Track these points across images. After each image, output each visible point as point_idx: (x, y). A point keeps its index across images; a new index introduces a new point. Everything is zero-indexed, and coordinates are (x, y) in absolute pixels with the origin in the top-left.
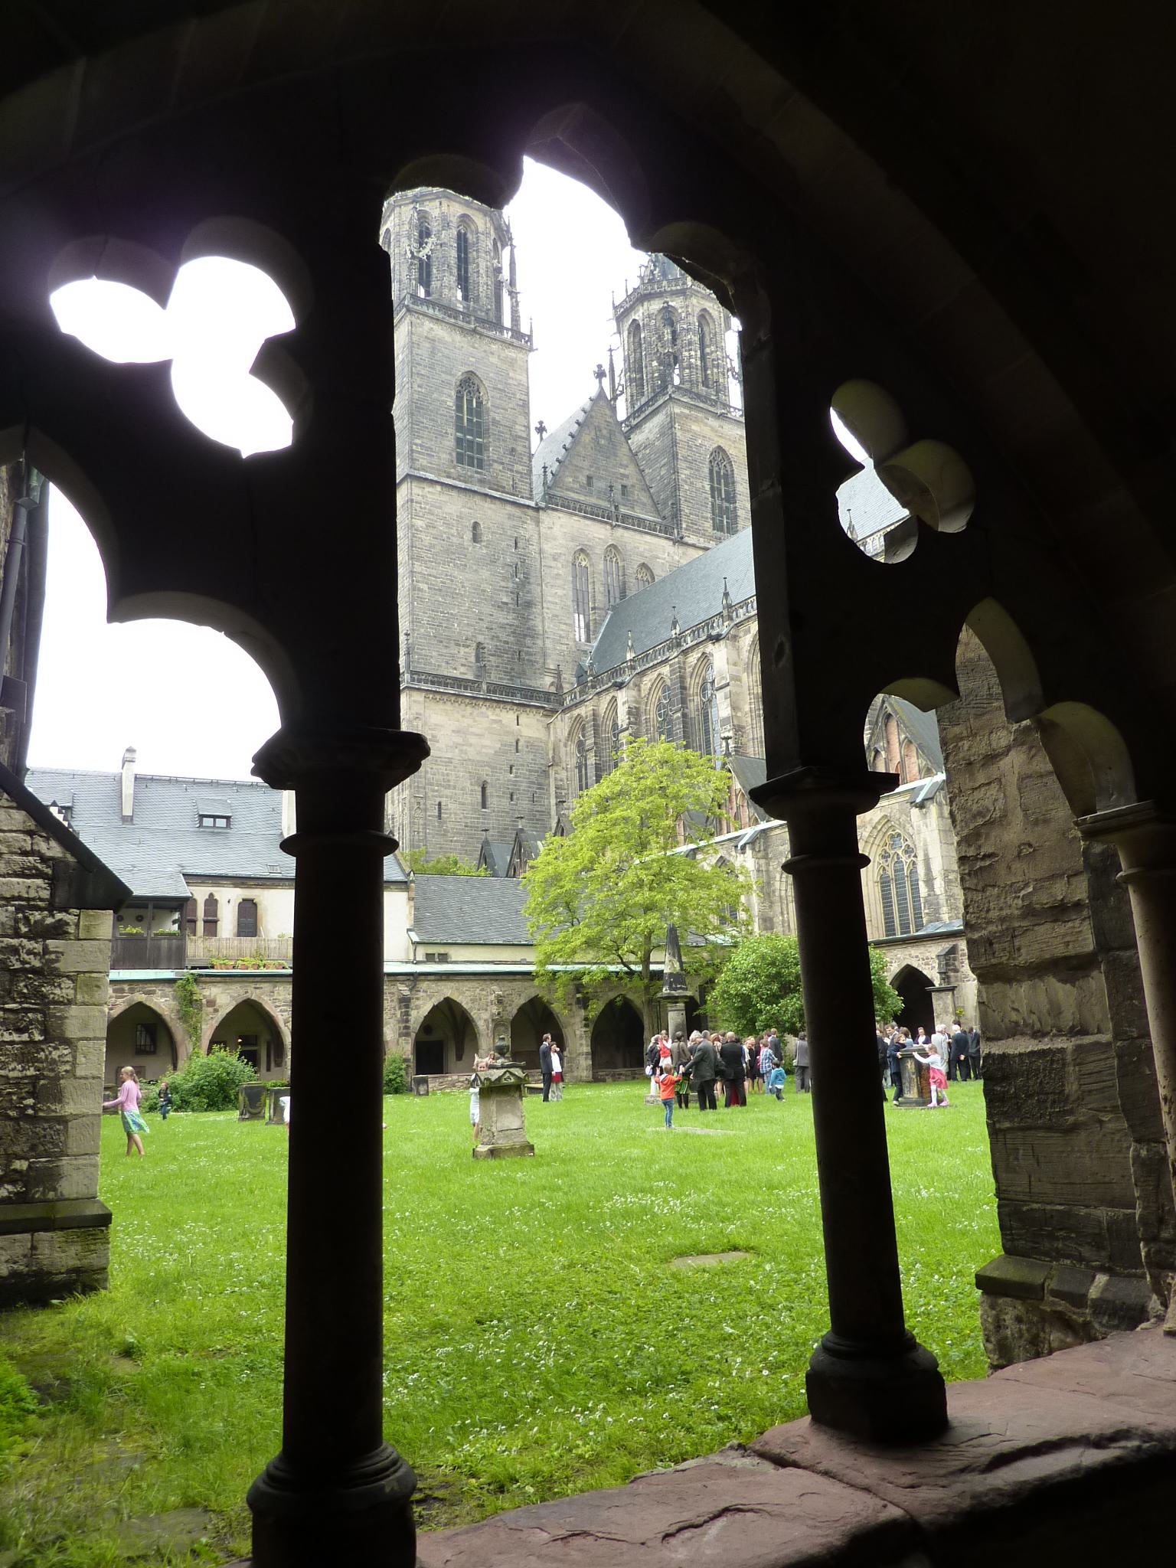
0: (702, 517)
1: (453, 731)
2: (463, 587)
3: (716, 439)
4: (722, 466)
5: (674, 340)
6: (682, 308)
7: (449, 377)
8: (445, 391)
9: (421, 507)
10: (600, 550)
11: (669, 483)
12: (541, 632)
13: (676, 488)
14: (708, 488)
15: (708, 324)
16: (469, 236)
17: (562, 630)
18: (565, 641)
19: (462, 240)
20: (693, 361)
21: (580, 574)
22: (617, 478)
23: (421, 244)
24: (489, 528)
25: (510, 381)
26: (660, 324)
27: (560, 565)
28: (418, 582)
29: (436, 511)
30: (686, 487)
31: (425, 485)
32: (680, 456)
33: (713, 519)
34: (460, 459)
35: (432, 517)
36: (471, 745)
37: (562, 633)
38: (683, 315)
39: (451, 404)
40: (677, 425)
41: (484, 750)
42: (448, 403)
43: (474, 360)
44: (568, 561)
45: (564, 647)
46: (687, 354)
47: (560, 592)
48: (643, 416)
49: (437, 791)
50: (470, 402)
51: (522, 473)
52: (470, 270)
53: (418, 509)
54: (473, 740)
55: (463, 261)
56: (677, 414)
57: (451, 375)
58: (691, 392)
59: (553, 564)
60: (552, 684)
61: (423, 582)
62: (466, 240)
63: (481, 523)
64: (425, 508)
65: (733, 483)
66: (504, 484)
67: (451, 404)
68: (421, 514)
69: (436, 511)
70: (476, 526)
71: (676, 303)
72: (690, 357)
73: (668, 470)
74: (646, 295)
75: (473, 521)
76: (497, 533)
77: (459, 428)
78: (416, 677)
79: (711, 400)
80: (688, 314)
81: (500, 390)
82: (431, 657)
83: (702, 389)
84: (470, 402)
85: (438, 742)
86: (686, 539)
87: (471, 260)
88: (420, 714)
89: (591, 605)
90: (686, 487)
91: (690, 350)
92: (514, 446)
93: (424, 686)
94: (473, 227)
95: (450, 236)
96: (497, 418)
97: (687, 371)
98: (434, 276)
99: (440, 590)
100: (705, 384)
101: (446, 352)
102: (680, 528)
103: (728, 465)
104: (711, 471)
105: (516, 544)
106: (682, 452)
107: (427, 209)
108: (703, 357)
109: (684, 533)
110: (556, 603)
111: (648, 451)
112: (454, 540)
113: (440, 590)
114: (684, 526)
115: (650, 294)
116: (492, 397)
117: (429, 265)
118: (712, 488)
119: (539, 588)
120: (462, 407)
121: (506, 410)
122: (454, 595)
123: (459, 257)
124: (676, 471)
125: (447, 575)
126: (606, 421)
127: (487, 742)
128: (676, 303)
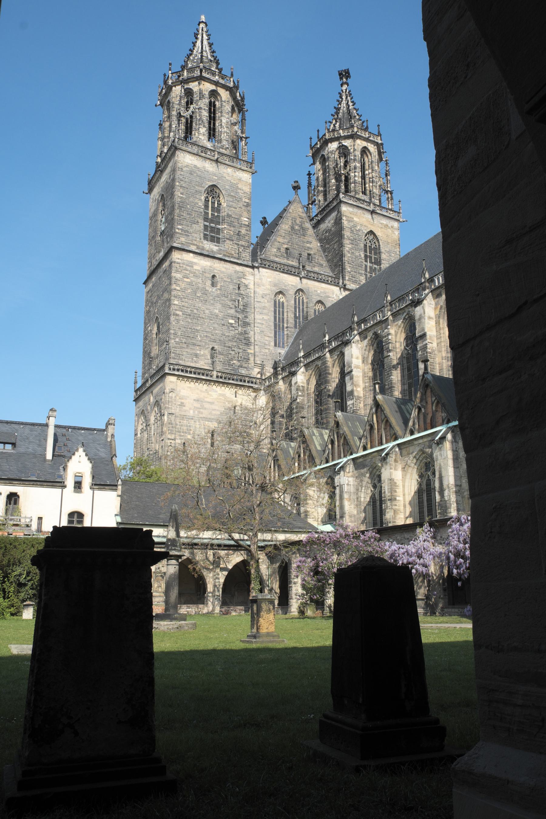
0: (359, 273)
1: (194, 400)
2: (204, 313)
3: (369, 226)
4: (373, 243)
5: (345, 166)
6: (351, 146)
7: (200, 189)
8: (197, 196)
9: (180, 266)
10: (292, 292)
11: (338, 253)
12: (253, 341)
13: (342, 256)
14: (363, 256)
15: (367, 157)
16: (217, 103)
17: (266, 340)
18: (266, 347)
19: (212, 105)
20: (356, 178)
21: (278, 307)
22: (305, 249)
23: (187, 108)
24: (222, 279)
25: (239, 191)
26: (337, 156)
27: (266, 301)
28: (176, 310)
29: (189, 268)
30: (349, 255)
31: (184, 253)
32: (345, 236)
33: (366, 275)
34: (205, 237)
35: (187, 272)
36: (205, 409)
37: (266, 342)
38: (352, 150)
39: (201, 205)
40: (344, 218)
41: (214, 412)
42: (199, 204)
43: (216, 178)
44: (271, 299)
45: (267, 351)
46: (353, 174)
47: (266, 317)
48: (325, 212)
49: (183, 436)
50: (213, 203)
51: (244, 246)
52: (217, 124)
53: (178, 267)
54: (207, 405)
55: (212, 118)
56: (345, 211)
57: (201, 187)
58: (354, 197)
59: (262, 300)
60: (259, 373)
61: (179, 311)
62: (215, 106)
63: (217, 275)
64: (183, 267)
65: (380, 253)
66: (233, 252)
67: (201, 205)
68: (180, 270)
69: (189, 268)
70: (214, 276)
71: (347, 143)
72: (355, 176)
73: (338, 245)
74: (329, 139)
75: (212, 274)
76: (227, 281)
77: (206, 219)
78: (172, 367)
79: (366, 202)
80: (355, 150)
81: (232, 196)
82: (183, 355)
83: (361, 196)
84: (213, 203)
85: (184, 406)
86: (347, 287)
87: (217, 118)
88: (174, 389)
89: (285, 325)
90: (349, 255)
91: (355, 172)
92: (240, 230)
93: (176, 373)
94: (219, 97)
95: (204, 103)
96: (230, 213)
97: (353, 185)
98: (193, 128)
99: (190, 315)
100: (364, 193)
101: (199, 173)
102: (343, 279)
103: (377, 243)
104: (365, 246)
105: (239, 288)
106: (347, 233)
107: (191, 87)
108: (363, 177)
109: (346, 282)
110: (263, 324)
111: (327, 234)
112: (200, 285)
113: (190, 315)
114: (347, 278)
115: (332, 138)
116: (227, 200)
117: (191, 122)
118: (366, 256)
119: (253, 314)
120: (208, 207)
121: (236, 208)
122: (198, 318)
123: (210, 116)
124: (341, 245)
125: (194, 306)
126: (299, 215)
127: (217, 408)
128: (347, 143)
